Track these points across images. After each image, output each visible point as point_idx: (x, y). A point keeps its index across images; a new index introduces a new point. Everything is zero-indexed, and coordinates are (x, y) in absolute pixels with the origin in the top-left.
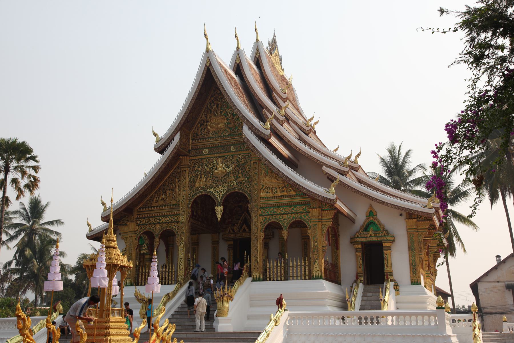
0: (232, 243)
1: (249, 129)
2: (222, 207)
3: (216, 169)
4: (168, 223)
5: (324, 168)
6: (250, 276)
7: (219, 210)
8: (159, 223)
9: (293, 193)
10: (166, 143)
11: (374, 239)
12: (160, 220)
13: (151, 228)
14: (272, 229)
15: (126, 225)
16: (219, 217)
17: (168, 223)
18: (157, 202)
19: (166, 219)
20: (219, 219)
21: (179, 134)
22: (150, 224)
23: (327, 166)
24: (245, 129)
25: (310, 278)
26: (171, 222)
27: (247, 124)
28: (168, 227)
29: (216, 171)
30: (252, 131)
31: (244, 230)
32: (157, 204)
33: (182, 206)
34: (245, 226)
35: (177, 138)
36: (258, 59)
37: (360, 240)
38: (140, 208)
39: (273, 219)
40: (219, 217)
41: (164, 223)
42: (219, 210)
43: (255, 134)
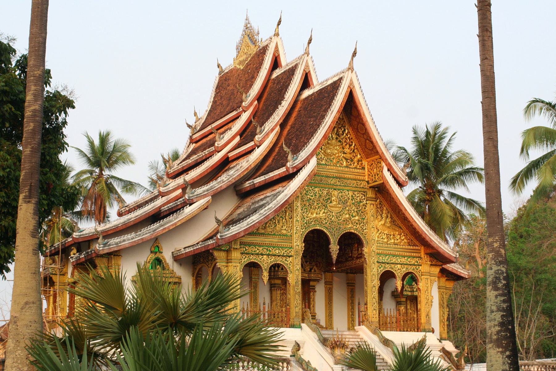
1: (388, 170)
2: (338, 247)
4: (279, 256)
7: (334, 249)
8: (268, 255)
12: (270, 251)
14: (386, 277)
16: (334, 257)
17: (279, 256)
19: (277, 251)
22: (258, 254)
26: (283, 256)
28: (279, 261)
29: (331, 205)
32: (263, 231)
35: (313, 161)
36: (276, 58)
40: (334, 257)
41: (275, 255)
42: (334, 249)
43: (393, 177)
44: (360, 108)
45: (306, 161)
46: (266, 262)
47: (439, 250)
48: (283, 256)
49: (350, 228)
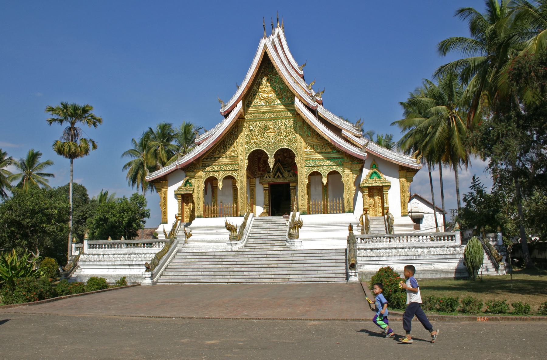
0: (267, 186)
1: (300, 101)
3: (268, 130)
5: (343, 132)
6: (298, 211)
7: (271, 162)
8: (222, 171)
9: (330, 150)
10: (230, 109)
11: (378, 185)
13: (216, 175)
14: (315, 175)
15: (193, 171)
16: (271, 166)
18: (219, 154)
20: (272, 168)
21: (241, 101)
22: (214, 171)
23: (345, 130)
24: (297, 101)
25: (343, 212)
26: (232, 170)
27: (297, 97)
29: (268, 131)
30: (302, 103)
31: (278, 177)
32: (218, 156)
33: (240, 158)
34: (278, 174)
37: (367, 185)
38: (205, 159)
39: (315, 169)
40: (271, 166)
41: (226, 171)
42: (271, 162)
43: (304, 105)
44: (273, 62)
45: (235, 105)
46: (220, 176)
47: (348, 152)
48: (232, 170)
49: (284, 145)
